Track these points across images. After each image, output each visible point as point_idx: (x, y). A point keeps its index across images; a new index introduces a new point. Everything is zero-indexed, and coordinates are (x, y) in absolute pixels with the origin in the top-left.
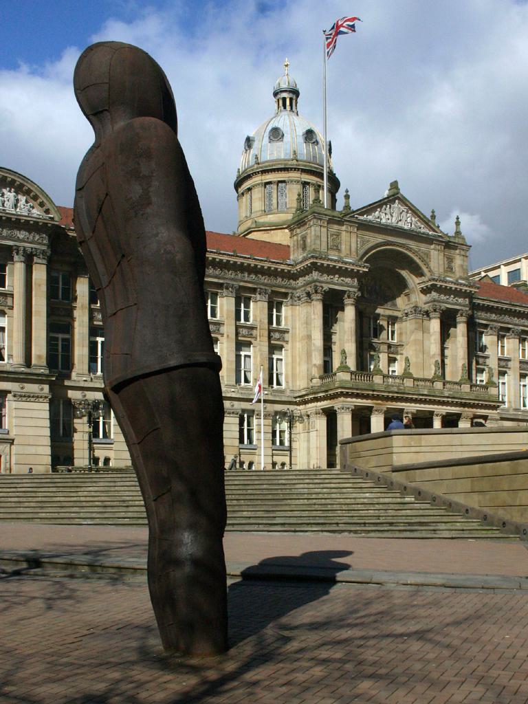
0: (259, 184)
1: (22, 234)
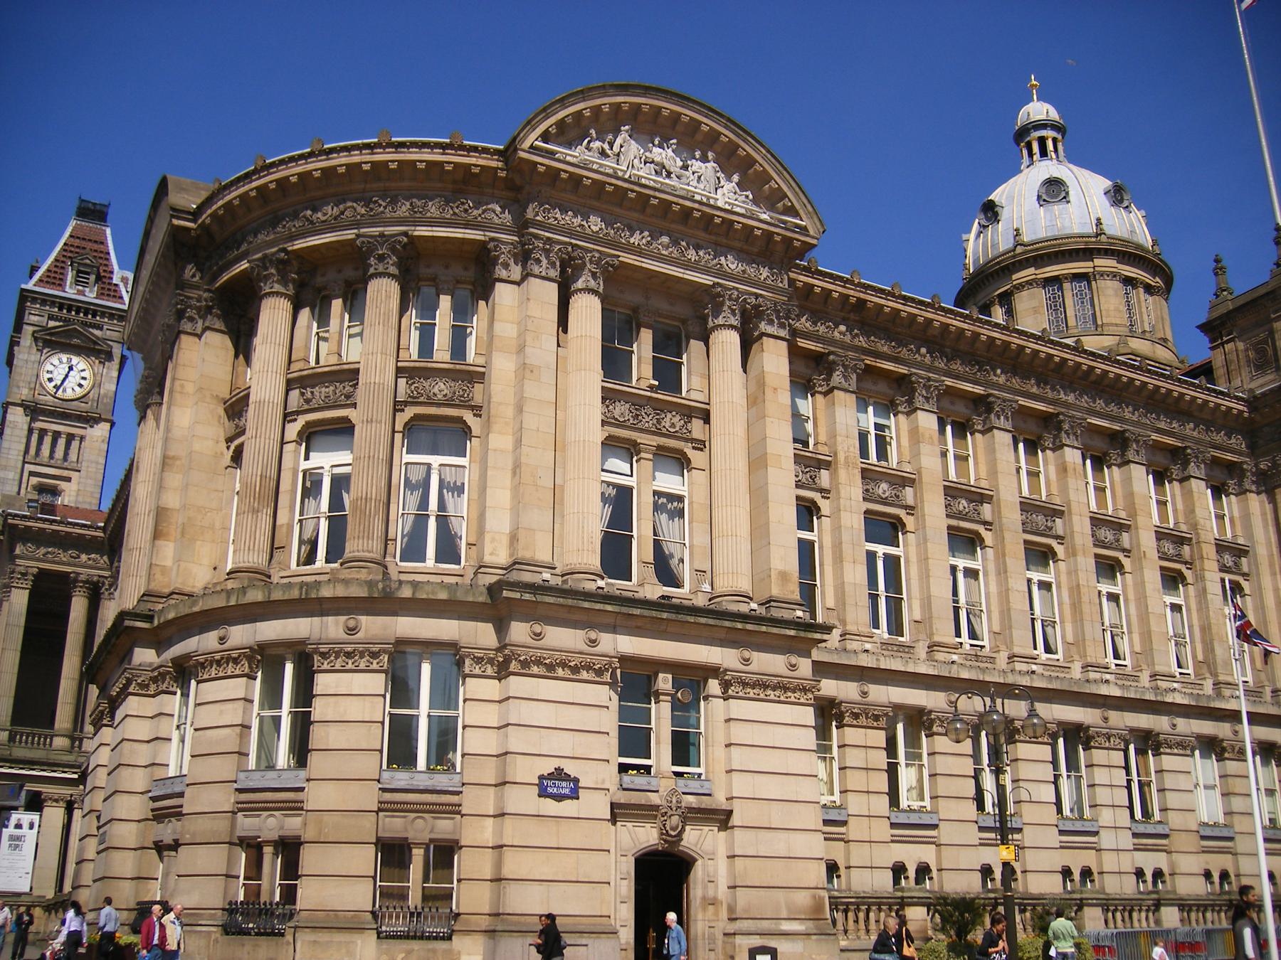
0: (1029, 283)
1: (731, 264)
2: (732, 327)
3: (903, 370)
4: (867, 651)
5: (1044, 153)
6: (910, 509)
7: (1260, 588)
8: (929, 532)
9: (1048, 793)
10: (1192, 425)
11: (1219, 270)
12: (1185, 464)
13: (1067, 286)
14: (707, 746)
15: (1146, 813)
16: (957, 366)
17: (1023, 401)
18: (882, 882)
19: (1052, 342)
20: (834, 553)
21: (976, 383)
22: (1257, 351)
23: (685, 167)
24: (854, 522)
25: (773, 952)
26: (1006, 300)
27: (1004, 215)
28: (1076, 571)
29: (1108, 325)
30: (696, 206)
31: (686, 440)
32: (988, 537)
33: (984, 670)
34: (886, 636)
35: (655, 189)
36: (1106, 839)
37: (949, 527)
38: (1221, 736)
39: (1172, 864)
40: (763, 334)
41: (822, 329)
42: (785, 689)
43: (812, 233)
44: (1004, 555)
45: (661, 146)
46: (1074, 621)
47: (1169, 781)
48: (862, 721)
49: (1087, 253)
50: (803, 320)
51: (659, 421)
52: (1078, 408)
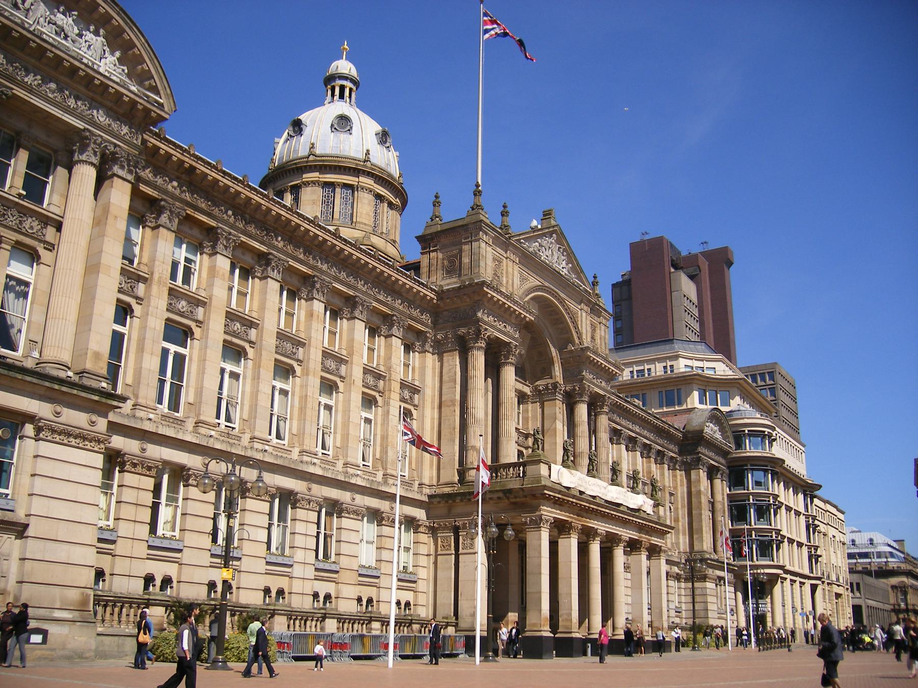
0: (314, 183)
1: (101, 117)
2: (92, 164)
3: (213, 223)
4: (150, 419)
5: (342, 96)
6: (199, 323)
7: (423, 416)
8: (210, 342)
9: (262, 535)
10: (400, 301)
11: (436, 203)
12: (391, 326)
13: (338, 190)
14: (16, 474)
15: (326, 556)
16: (251, 229)
17: (292, 262)
18: (136, 587)
19: (320, 226)
20: (138, 344)
21: (262, 243)
22: (450, 262)
23: (80, 35)
24: (157, 325)
25: (45, 633)
26: (296, 190)
27: (307, 131)
28: (306, 386)
29: (360, 223)
30: (83, 67)
31: (40, 241)
32: (251, 352)
33: (232, 445)
34: (166, 410)
35: (53, 45)
36: (297, 571)
37: (225, 341)
38: (382, 510)
39: (338, 591)
40: (114, 175)
41: (159, 181)
42: (84, 438)
43: (166, 109)
44: (259, 367)
45: (64, 14)
46: (299, 420)
47: (345, 536)
48: (139, 469)
49: (356, 172)
50: (147, 171)
51: (21, 222)
52: (329, 275)
